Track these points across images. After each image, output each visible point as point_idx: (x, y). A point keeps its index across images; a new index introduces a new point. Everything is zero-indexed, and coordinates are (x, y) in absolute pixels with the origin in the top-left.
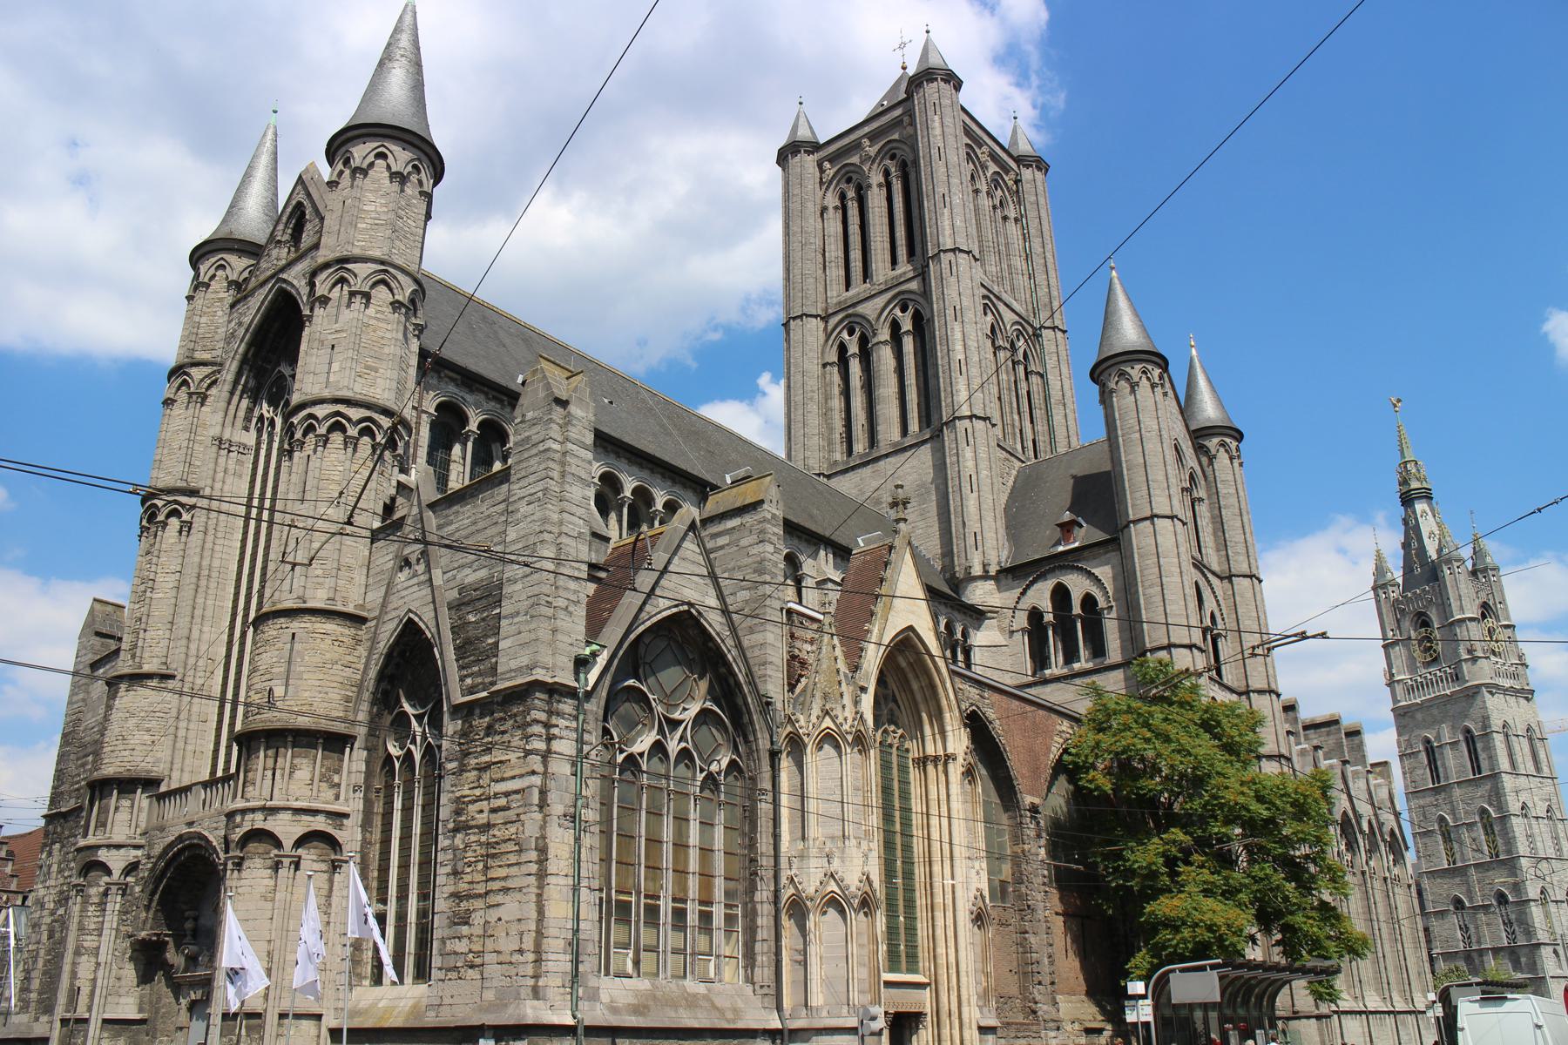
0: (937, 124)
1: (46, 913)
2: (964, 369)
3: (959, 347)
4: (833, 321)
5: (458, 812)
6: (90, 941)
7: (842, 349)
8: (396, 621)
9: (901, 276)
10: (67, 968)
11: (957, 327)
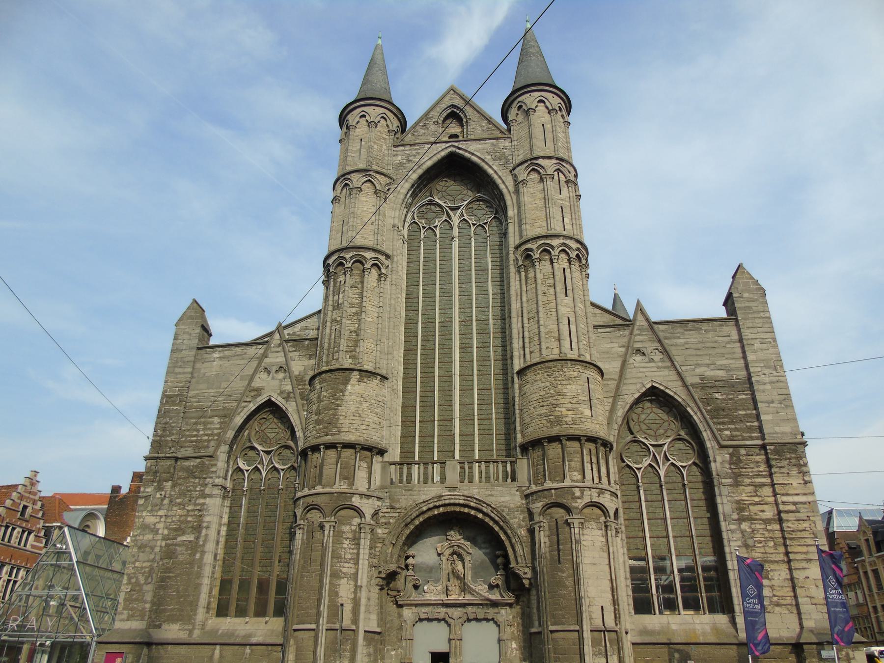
1: (159, 537)
5: (740, 510)
6: (348, 568)
8: (638, 386)
10: (327, 588)
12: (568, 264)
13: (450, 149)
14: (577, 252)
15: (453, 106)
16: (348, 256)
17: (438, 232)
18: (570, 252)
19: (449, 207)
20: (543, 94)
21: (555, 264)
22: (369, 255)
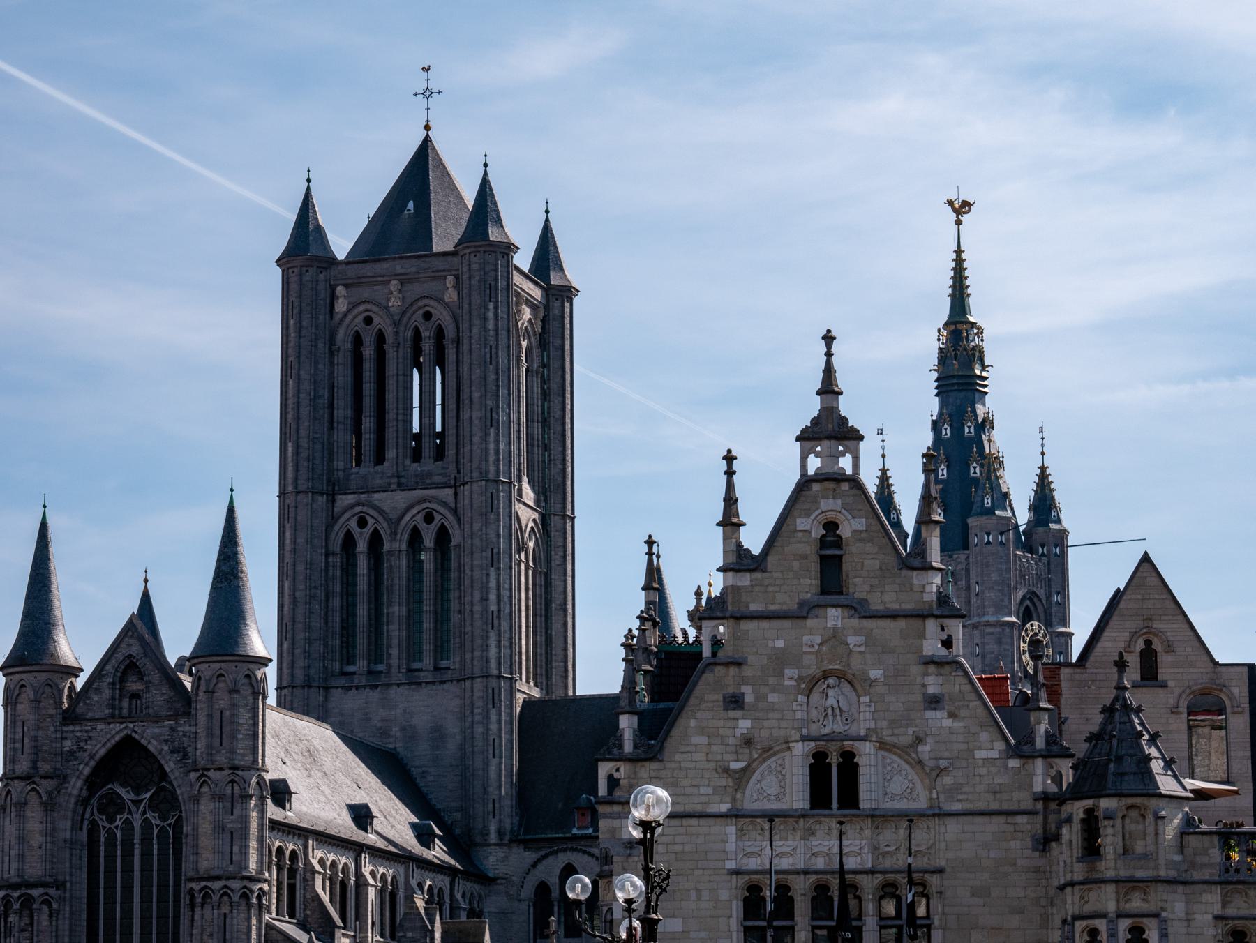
0: (491, 315)
2: (496, 622)
3: (493, 597)
4: (344, 500)
7: (349, 540)
9: (429, 474)
11: (492, 572)
12: (230, 908)
13: (125, 732)
14: (242, 891)
15: (130, 656)
16: (16, 894)
17: (118, 834)
18: (232, 895)
19: (132, 801)
20: (223, 664)
21: (215, 911)
22: (36, 892)
